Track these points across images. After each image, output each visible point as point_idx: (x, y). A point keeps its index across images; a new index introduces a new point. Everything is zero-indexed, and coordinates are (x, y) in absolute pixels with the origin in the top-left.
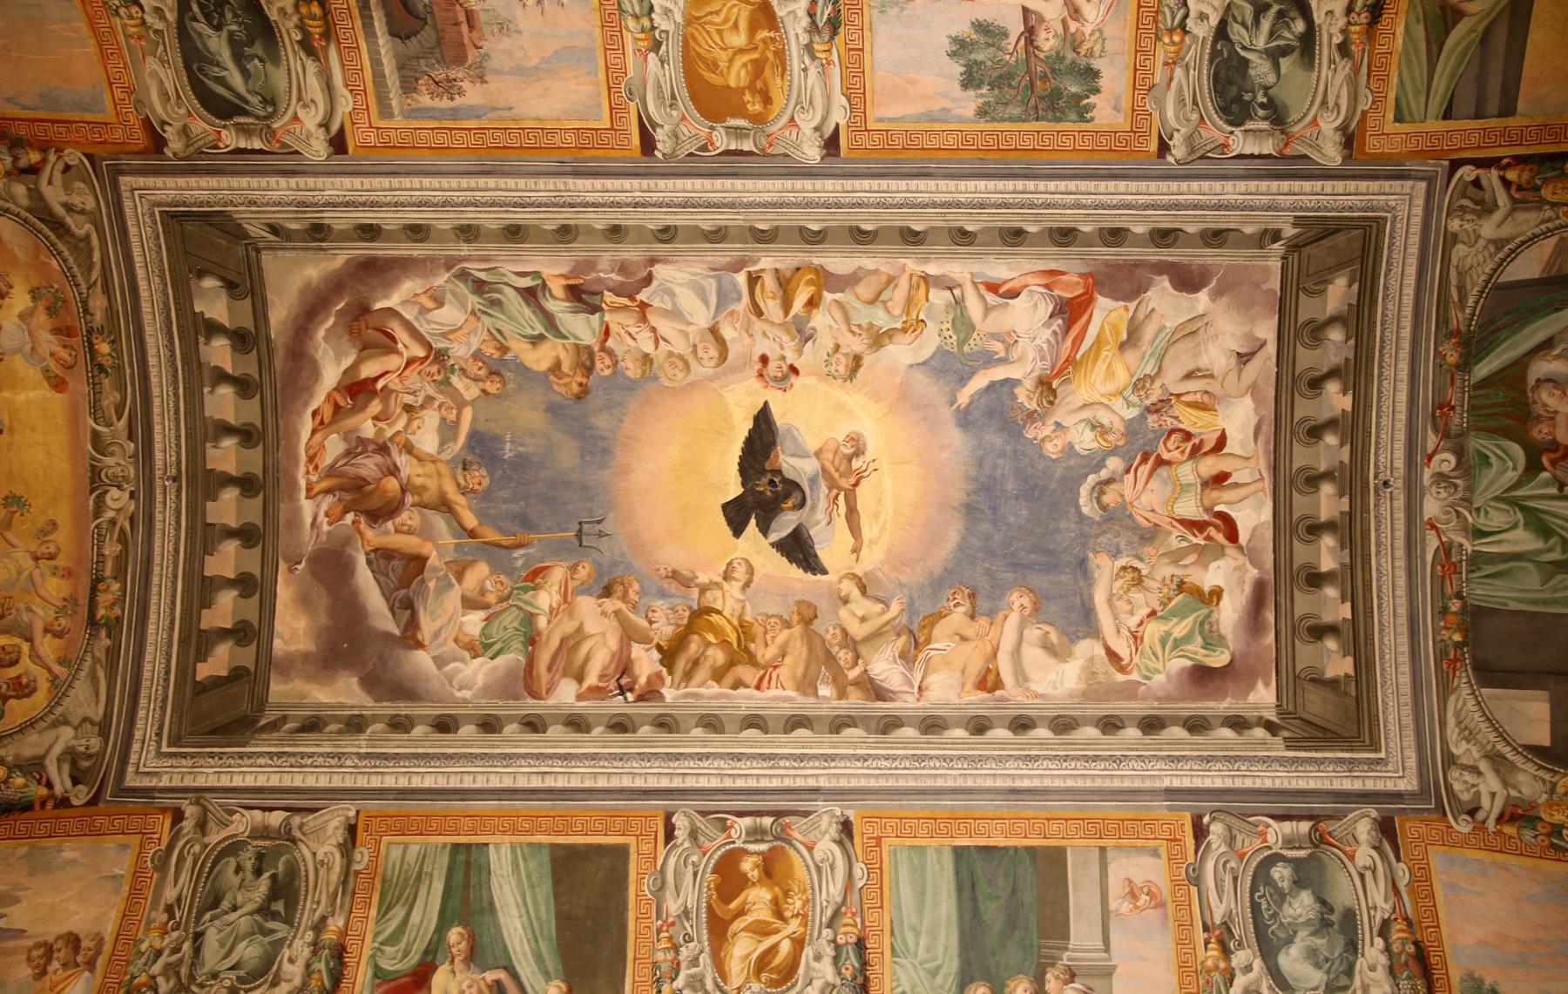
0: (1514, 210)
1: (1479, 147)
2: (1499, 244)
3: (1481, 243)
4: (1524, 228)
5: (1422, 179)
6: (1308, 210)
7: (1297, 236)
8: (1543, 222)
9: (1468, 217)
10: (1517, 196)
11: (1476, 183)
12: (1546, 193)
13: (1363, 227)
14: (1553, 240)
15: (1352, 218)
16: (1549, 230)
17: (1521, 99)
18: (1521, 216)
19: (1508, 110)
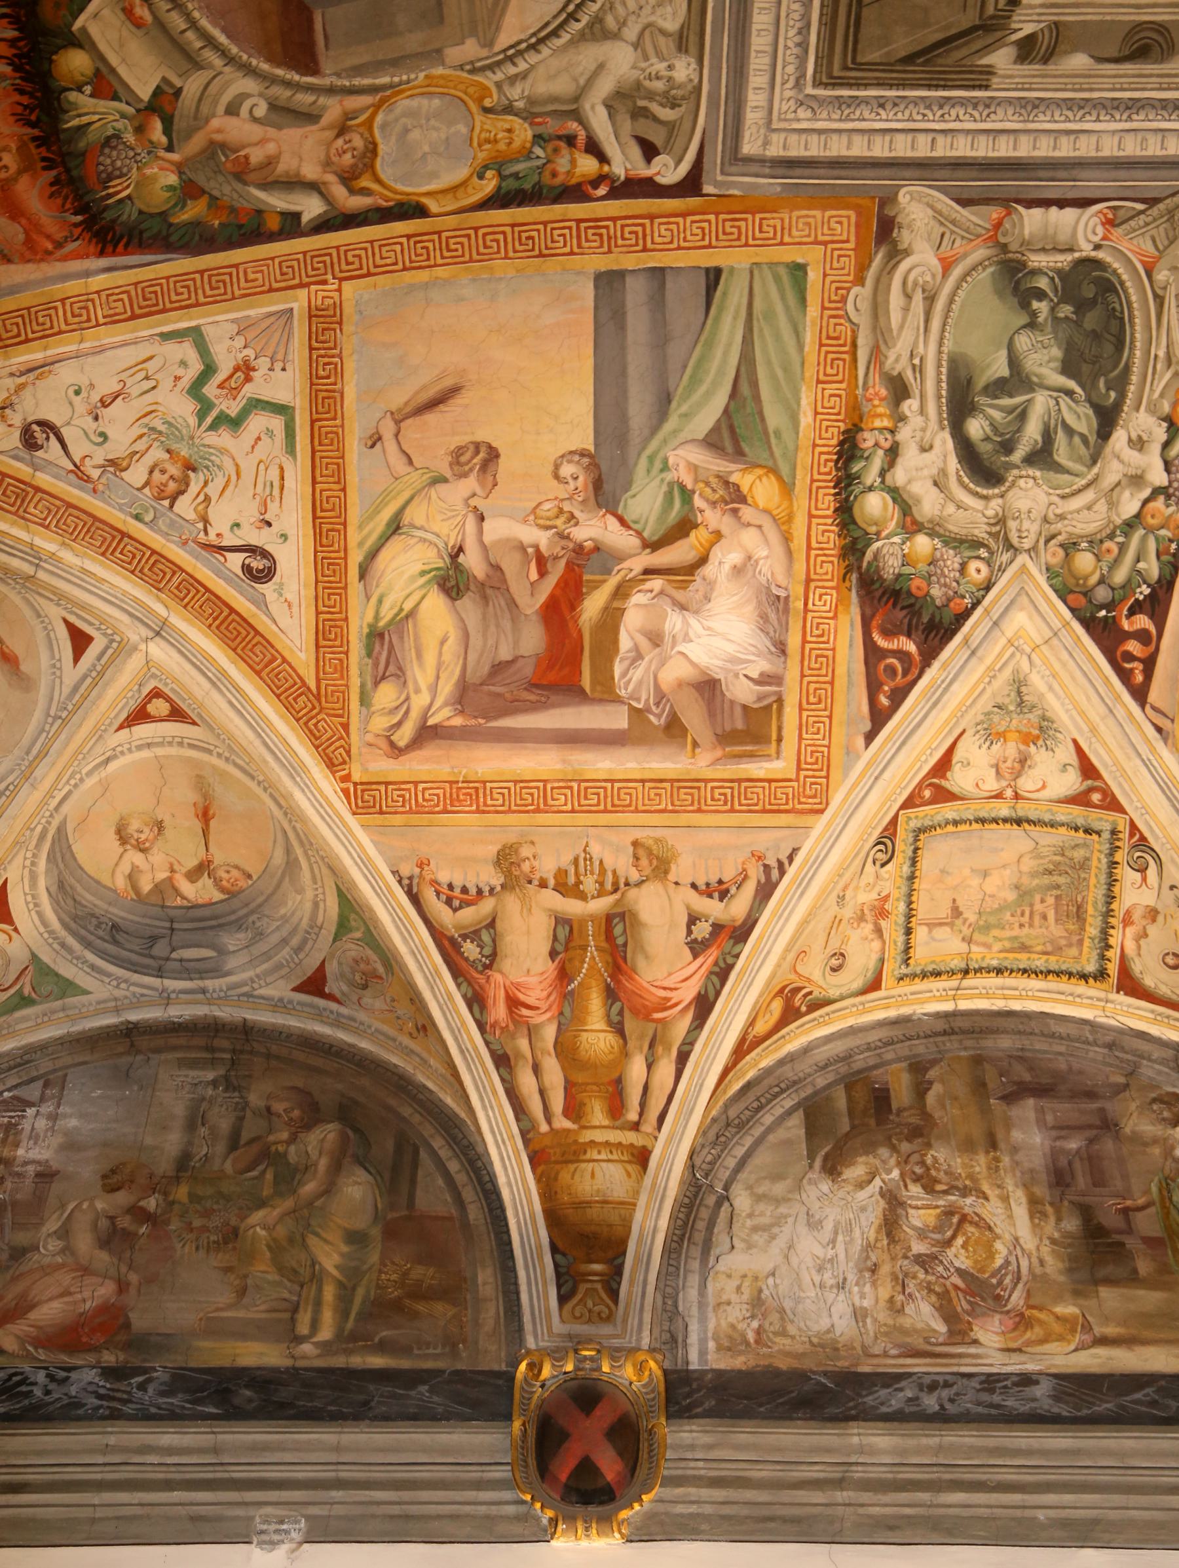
0: (576, 99)
1: (652, 217)
2: (598, 32)
3: (631, 33)
4: (555, 63)
5: (749, 160)
6: (962, 102)
7: (987, 49)
8: (524, 76)
9: (659, 86)
10: (574, 126)
11: (649, 151)
12: (524, 133)
13: (859, 66)
14: (504, 39)
15: (880, 84)
16: (511, 59)
17: (590, 303)
18: (562, 86)
19: (609, 283)
